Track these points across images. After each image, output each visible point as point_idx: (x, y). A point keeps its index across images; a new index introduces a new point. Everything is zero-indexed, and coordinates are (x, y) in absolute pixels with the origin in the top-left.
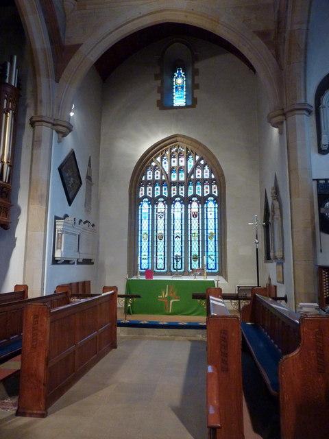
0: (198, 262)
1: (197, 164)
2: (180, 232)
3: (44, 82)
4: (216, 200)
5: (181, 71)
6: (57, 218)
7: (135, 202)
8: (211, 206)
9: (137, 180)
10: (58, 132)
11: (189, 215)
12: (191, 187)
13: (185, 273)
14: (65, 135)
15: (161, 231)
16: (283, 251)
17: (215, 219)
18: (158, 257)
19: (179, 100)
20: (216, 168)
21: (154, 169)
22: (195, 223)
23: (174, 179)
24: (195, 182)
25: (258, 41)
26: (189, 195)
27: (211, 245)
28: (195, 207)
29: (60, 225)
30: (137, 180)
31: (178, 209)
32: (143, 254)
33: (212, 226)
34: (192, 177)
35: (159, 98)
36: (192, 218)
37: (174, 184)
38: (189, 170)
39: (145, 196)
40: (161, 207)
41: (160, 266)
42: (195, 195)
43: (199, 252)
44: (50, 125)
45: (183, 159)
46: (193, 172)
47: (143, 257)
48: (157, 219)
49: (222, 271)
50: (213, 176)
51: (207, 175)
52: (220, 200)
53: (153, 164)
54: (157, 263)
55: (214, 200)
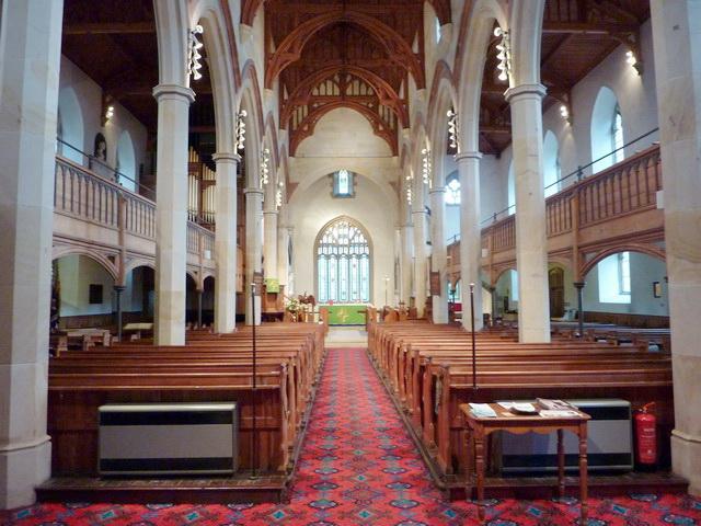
1: (356, 233)
7: (317, 257)
8: (365, 262)
9: (317, 245)
19: (343, 188)
20: (367, 236)
22: (354, 272)
23: (341, 242)
25: (391, 188)
27: (365, 285)
28: (354, 261)
31: (343, 261)
49: (371, 301)
51: (361, 239)
52: (370, 257)
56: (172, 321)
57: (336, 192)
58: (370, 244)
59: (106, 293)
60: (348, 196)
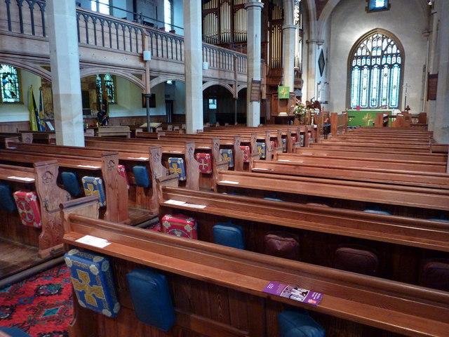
1: (389, 44)
3: (313, 23)
4: (399, 65)
7: (350, 69)
8: (396, 70)
9: (352, 55)
12: (384, 59)
13: (378, 108)
20: (400, 47)
22: (385, 81)
23: (374, 54)
24: (387, 55)
27: (395, 93)
29: (320, 87)
30: (352, 55)
31: (376, 71)
33: (396, 81)
34: (385, 53)
37: (374, 57)
40: (366, 71)
41: (364, 104)
45: (380, 41)
46: (386, 49)
50: (398, 52)
51: (395, 50)
52: (401, 66)
53: (362, 46)
56: (63, 123)
57: (372, 6)
58: (402, 54)
59: (160, 100)
60: (383, 9)
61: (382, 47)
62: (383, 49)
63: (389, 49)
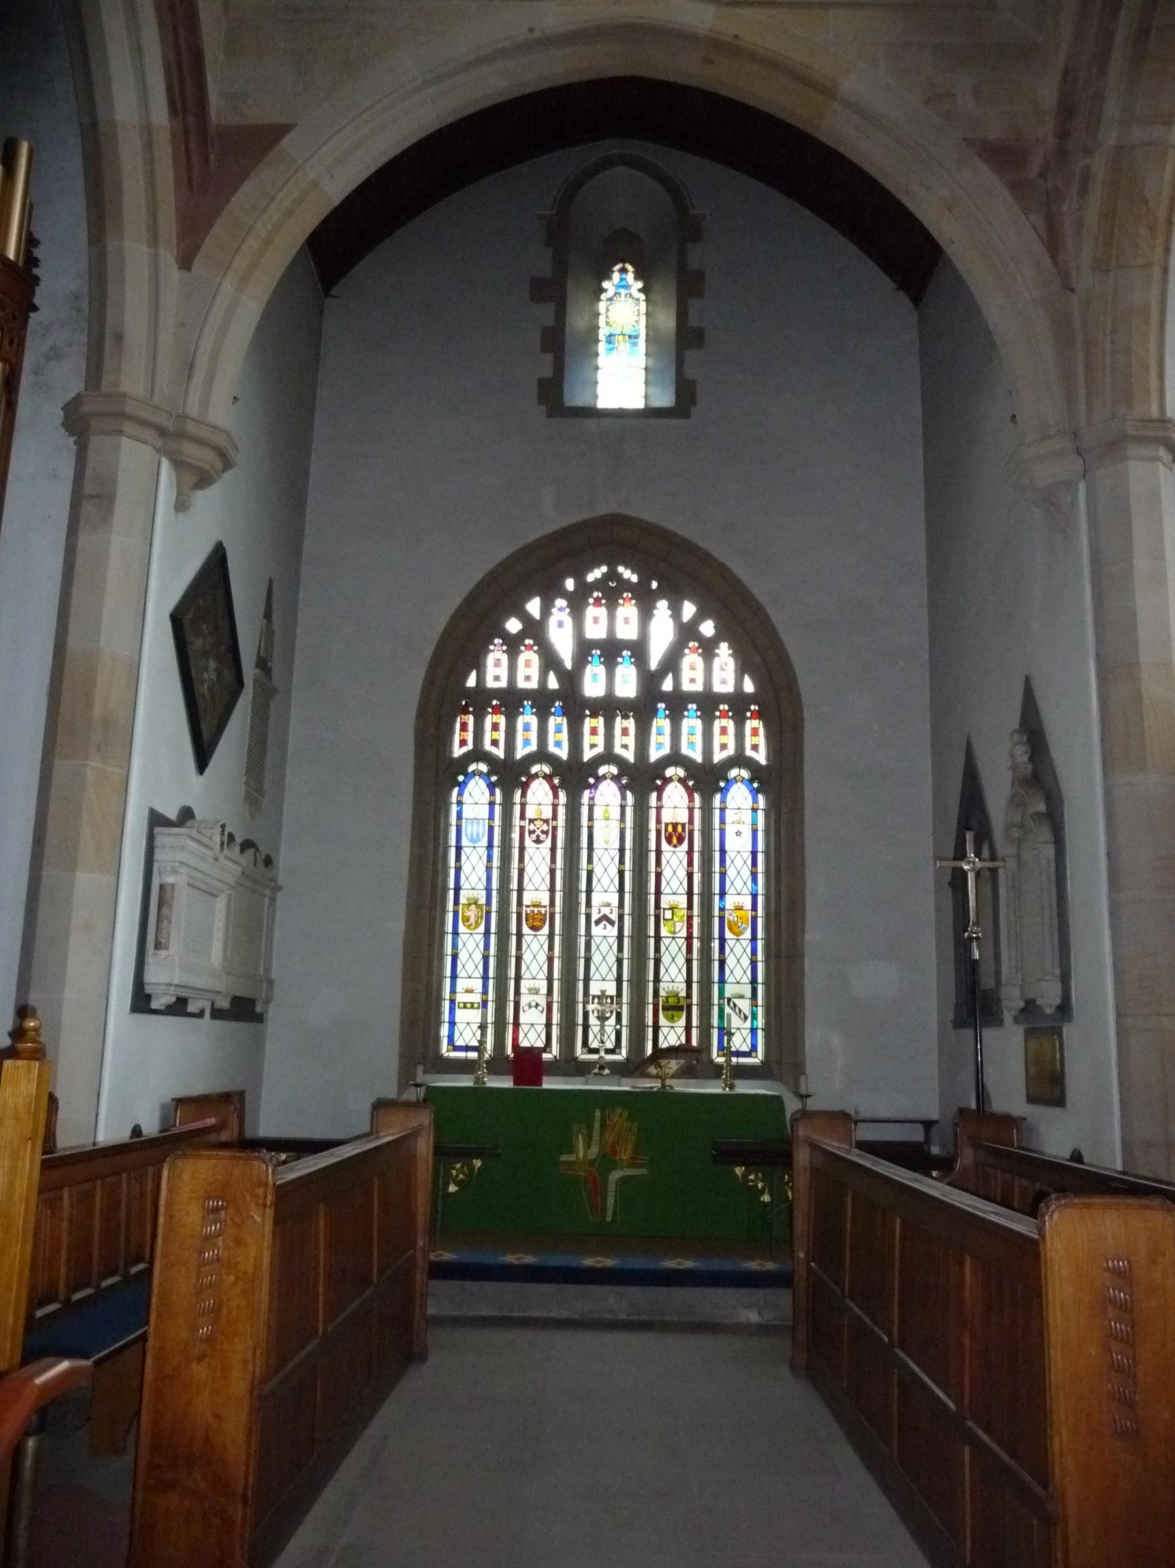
0: (682, 1022)
1: (686, 633)
2: (614, 899)
4: (761, 779)
5: (630, 276)
6: (156, 820)
10: (178, 464)
11: (653, 836)
12: (661, 724)
14: (204, 480)
15: (536, 893)
16: (1065, 979)
17: (754, 854)
18: (525, 1000)
21: (513, 645)
23: (593, 685)
24: (677, 704)
26: (654, 755)
32: (461, 984)
34: (667, 685)
35: (548, 372)
36: (665, 845)
38: (655, 657)
39: (478, 754)
42: (676, 758)
43: (689, 982)
44: (149, 434)
46: (672, 663)
47: (460, 998)
48: (522, 849)
50: (749, 686)
54: (517, 1024)
55: (751, 781)
61: (639, 650)
62: (654, 662)
63: (692, 663)
